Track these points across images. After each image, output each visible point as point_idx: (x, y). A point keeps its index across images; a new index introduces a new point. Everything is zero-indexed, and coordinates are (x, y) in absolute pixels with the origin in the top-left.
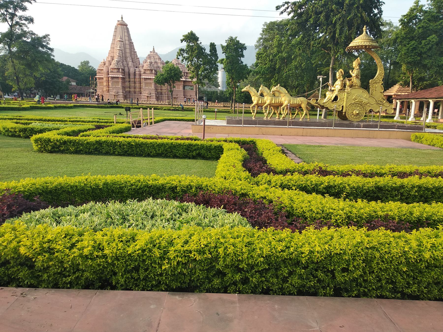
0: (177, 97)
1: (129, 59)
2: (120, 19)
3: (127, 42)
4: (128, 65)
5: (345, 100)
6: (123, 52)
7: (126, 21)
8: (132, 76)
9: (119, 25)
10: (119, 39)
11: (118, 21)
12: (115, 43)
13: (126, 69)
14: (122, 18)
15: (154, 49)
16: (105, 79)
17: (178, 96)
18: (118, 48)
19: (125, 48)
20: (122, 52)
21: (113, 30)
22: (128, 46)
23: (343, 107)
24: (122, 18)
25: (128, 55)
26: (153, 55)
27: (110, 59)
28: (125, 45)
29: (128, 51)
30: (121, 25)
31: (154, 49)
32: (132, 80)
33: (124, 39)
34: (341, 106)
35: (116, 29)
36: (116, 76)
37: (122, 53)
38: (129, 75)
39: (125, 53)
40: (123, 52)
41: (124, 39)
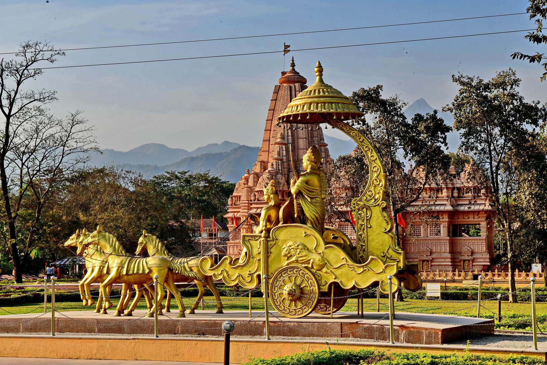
0: (430, 258)
5: (261, 257)
9: (284, 82)
11: (284, 73)
14: (293, 65)
17: (434, 256)
18: (278, 140)
21: (270, 95)
23: (259, 276)
24: (293, 65)
30: (289, 81)
34: (255, 275)
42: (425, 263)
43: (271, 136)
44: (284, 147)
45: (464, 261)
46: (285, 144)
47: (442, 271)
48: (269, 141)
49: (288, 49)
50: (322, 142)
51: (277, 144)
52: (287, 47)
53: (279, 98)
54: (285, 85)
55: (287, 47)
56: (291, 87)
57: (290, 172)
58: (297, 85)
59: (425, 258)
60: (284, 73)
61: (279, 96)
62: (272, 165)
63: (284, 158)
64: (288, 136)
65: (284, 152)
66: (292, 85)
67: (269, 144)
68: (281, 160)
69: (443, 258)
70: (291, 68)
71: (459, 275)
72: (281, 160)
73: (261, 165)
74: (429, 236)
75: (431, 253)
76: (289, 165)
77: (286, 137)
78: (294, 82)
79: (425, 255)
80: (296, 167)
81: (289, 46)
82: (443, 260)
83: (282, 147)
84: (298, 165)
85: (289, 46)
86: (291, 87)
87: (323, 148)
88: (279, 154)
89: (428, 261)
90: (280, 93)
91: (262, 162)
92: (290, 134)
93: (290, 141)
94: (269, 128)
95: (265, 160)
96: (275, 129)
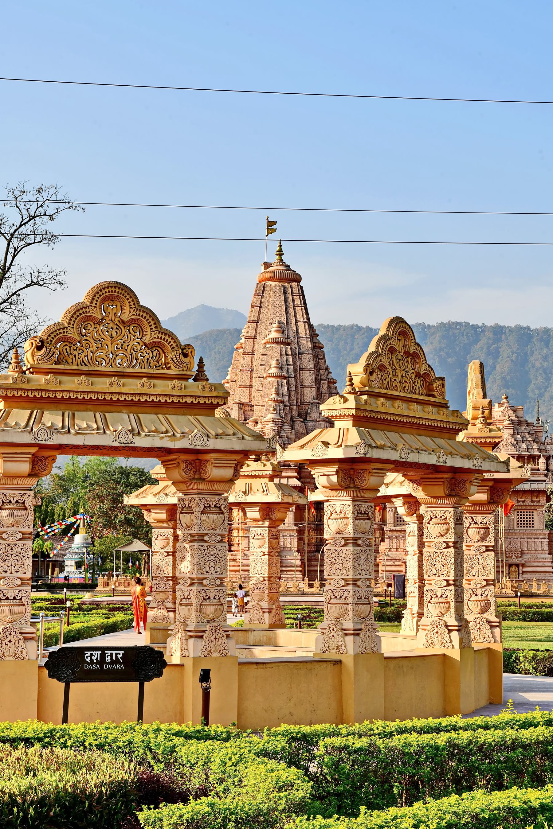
3: (306, 345)
6: (293, 386)
10: (274, 335)
11: (267, 265)
12: (259, 351)
14: (280, 253)
17: (527, 557)
18: (274, 371)
19: (298, 369)
20: (288, 384)
22: (308, 361)
24: (280, 253)
28: (297, 354)
29: (308, 378)
33: (292, 334)
35: (261, 292)
37: (289, 389)
40: (293, 386)
41: (292, 334)
42: (513, 568)
43: (255, 363)
44: (285, 381)
46: (285, 378)
47: (541, 581)
48: (252, 371)
49: (274, 227)
50: (329, 376)
51: (273, 377)
52: (271, 224)
53: (265, 305)
54: (273, 283)
55: (271, 224)
56: (284, 288)
57: (293, 421)
58: (294, 285)
59: (514, 561)
60: (267, 265)
61: (265, 299)
62: (274, 410)
63: (286, 399)
64: (288, 365)
65: (286, 390)
66: (286, 284)
67: (251, 376)
68: (282, 402)
69: (540, 561)
70: (277, 257)
71: (311, 586)
72: (282, 402)
73: (240, 409)
74: (516, 528)
75: (522, 553)
76: (291, 411)
77: (284, 366)
78: (290, 281)
79: (514, 557)
80: (299, 415)
81: (275, 223)
82: (540, 564)
83: (282, 382)
84: (303, 412)
85: (275, 223)
86: (284, 288)
87: (333, 386)
88: (278, 394)
89: (517, 565)
90: (266, 294)
91: (240, 404)
92: (291, 363)
93: (292, 373)
94: (249, 349)
95: (246, 400)
96: (265, 353)
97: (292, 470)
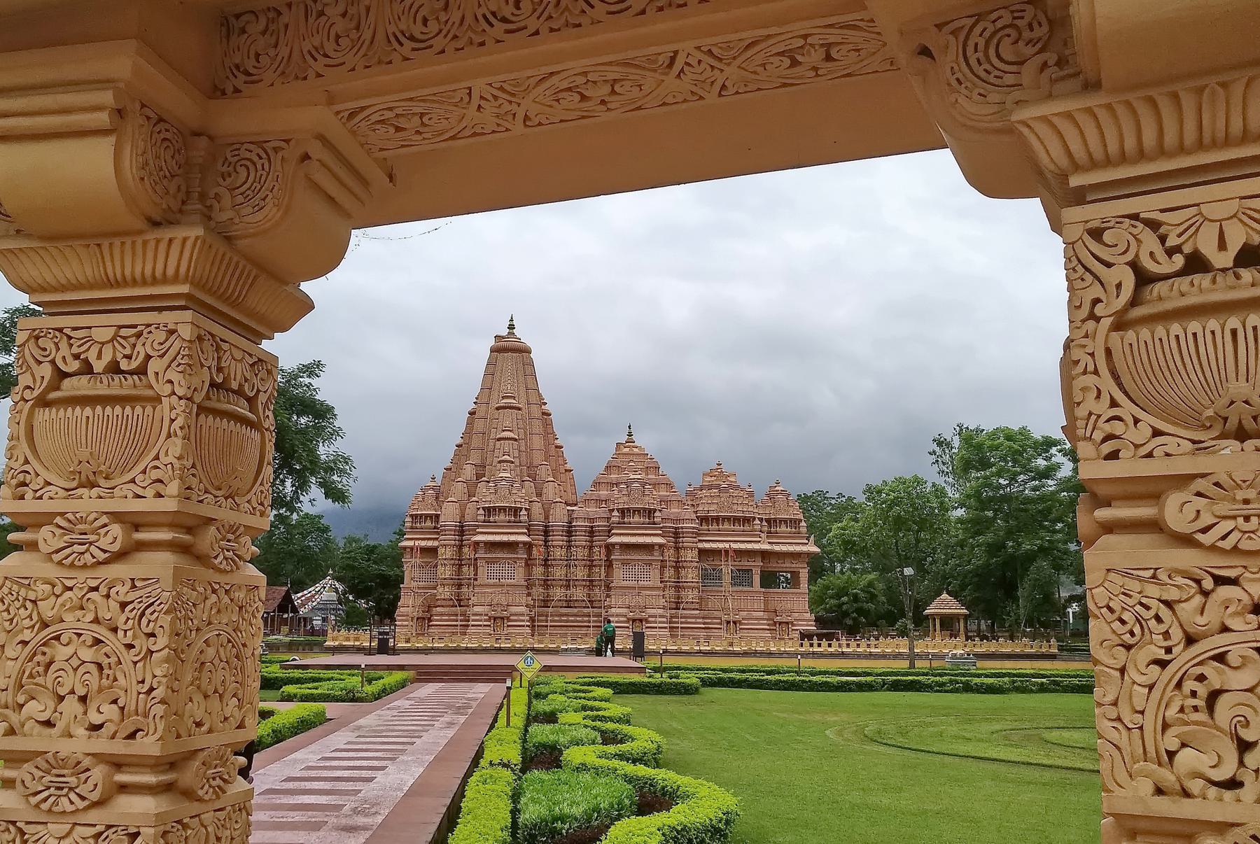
1: (544, 473)
2: (505, 332)
4: (539, 495)
7: (524, 335)
8: (558, 540)
13: (537, 509)
14: (511, 327)
15: (630, 435)
16: (446, 553)
22: (537, 426)
24: (511, 327)
25: (538, 458)
26: (627, 454)
27: (469, 472)
29: (538, 442)
31: (630, 435)
32: (559, 553)
36: (505, 538)
38: (546, 533)
39: (530, 451)
41: (523, 400)
45: (780, 623)
93: (522, 436)
95: (478, 462)
97: (522, 527)
